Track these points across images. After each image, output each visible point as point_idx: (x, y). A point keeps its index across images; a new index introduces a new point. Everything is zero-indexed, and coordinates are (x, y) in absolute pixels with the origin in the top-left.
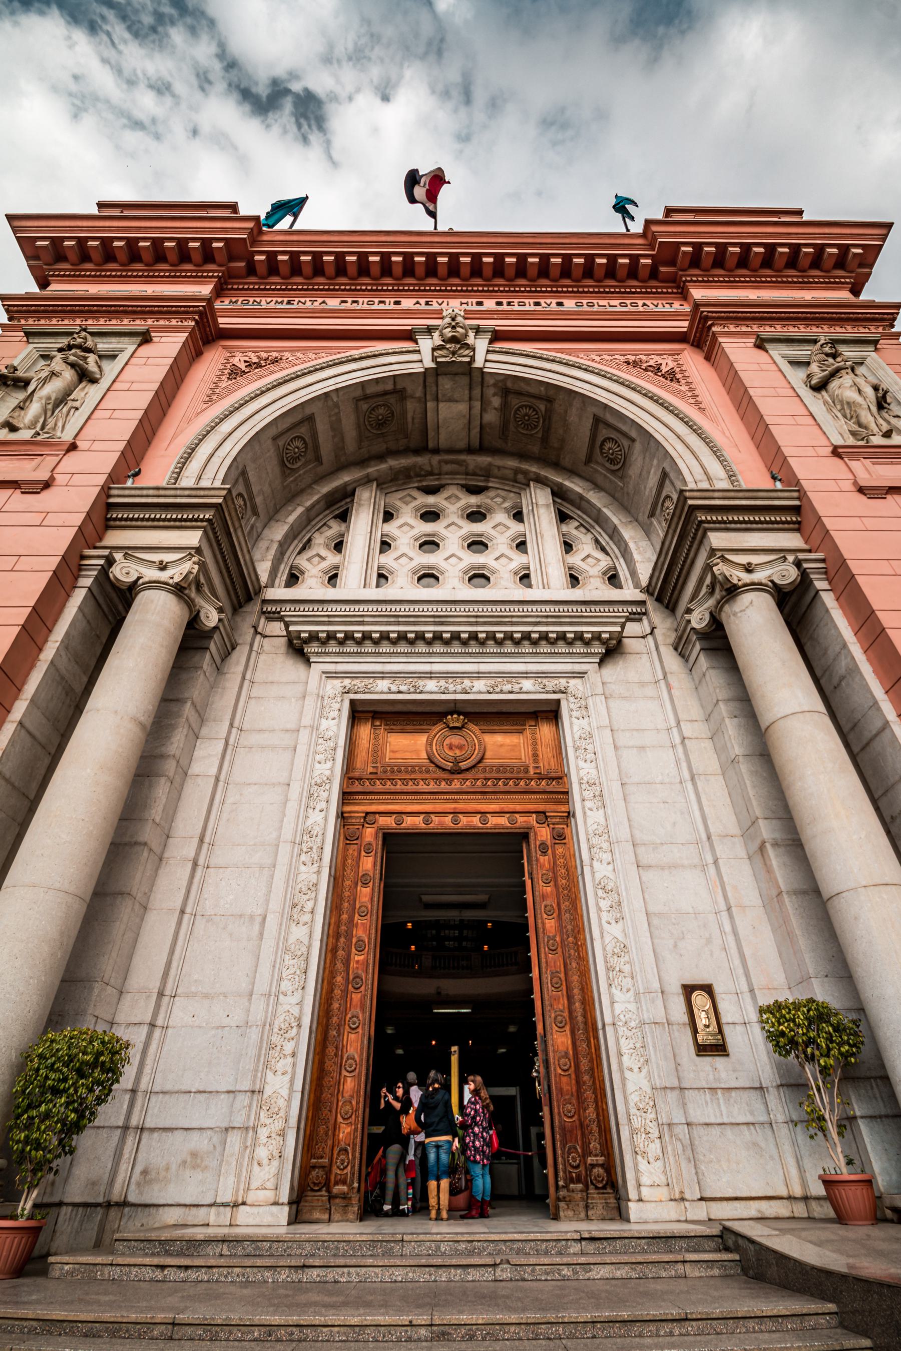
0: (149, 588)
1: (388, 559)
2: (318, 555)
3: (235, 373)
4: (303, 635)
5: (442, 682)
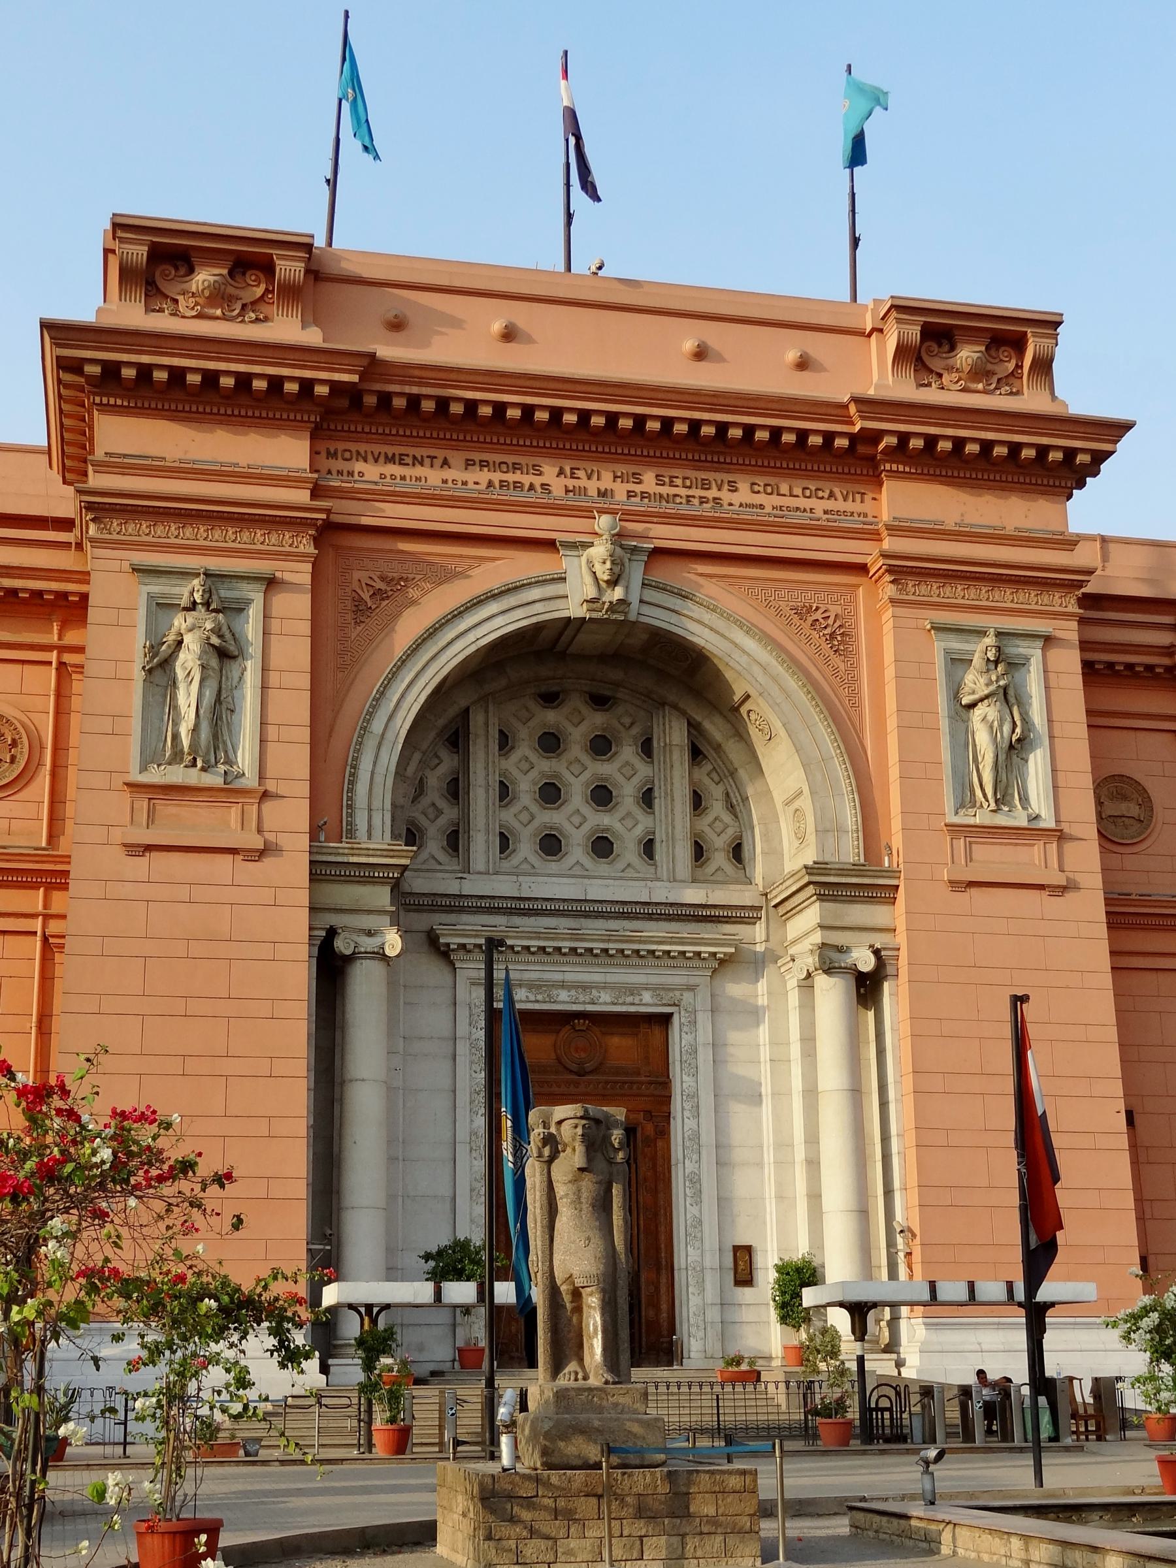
0: (366, 958)
1: (508, 816)
2: (434, 804)
3: (360, 610)
4: (452, 947)
5: (573, 992)
